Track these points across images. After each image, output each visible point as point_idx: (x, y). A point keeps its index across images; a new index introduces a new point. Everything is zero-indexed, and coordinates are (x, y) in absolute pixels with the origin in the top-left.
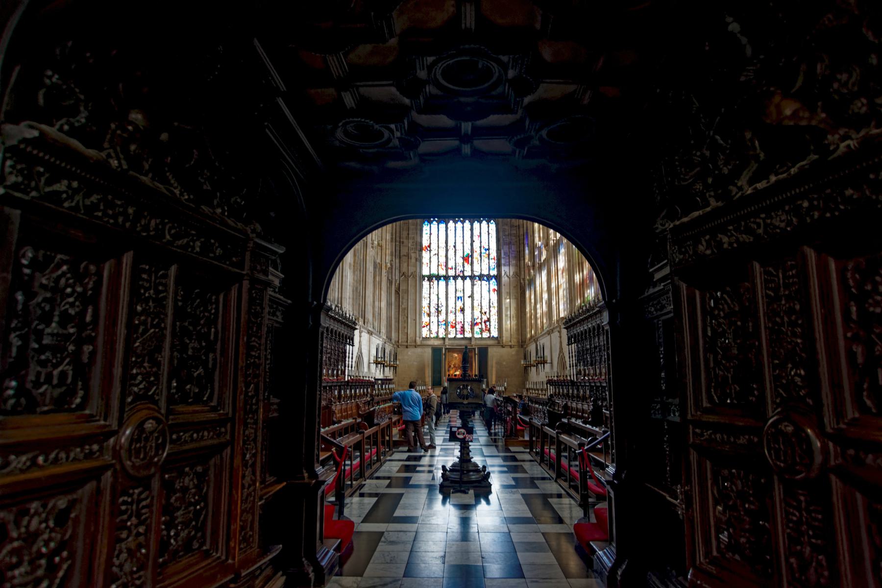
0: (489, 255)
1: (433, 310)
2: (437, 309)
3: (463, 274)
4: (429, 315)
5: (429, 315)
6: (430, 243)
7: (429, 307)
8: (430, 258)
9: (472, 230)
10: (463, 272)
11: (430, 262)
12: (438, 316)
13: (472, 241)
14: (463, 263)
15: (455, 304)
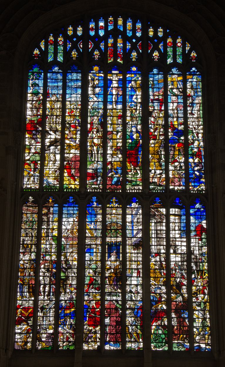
0: (187, 145)
1: (44, 278)
2: (56, 276)
3: (124, 189)
4: (35, 291)
5: (35, 291)
6: (44, 116)
7: (36, 271)
8: (43, 149)
9: (145, 87)
10: (124, 182)
11: (43, 159)
12: (57, 294)
13: (146, 114)
14: (123, 164)
15: (103, 261)
